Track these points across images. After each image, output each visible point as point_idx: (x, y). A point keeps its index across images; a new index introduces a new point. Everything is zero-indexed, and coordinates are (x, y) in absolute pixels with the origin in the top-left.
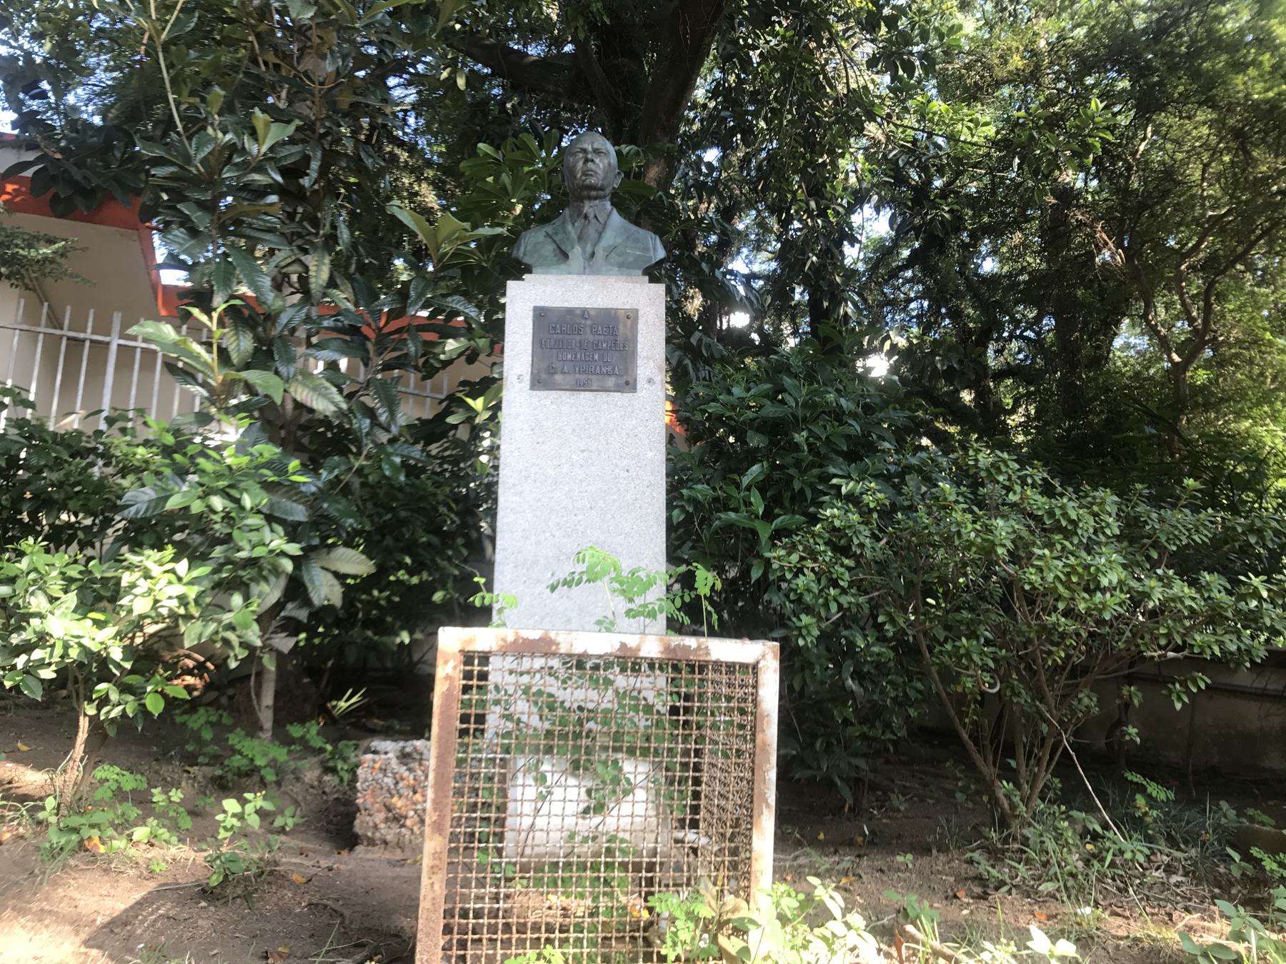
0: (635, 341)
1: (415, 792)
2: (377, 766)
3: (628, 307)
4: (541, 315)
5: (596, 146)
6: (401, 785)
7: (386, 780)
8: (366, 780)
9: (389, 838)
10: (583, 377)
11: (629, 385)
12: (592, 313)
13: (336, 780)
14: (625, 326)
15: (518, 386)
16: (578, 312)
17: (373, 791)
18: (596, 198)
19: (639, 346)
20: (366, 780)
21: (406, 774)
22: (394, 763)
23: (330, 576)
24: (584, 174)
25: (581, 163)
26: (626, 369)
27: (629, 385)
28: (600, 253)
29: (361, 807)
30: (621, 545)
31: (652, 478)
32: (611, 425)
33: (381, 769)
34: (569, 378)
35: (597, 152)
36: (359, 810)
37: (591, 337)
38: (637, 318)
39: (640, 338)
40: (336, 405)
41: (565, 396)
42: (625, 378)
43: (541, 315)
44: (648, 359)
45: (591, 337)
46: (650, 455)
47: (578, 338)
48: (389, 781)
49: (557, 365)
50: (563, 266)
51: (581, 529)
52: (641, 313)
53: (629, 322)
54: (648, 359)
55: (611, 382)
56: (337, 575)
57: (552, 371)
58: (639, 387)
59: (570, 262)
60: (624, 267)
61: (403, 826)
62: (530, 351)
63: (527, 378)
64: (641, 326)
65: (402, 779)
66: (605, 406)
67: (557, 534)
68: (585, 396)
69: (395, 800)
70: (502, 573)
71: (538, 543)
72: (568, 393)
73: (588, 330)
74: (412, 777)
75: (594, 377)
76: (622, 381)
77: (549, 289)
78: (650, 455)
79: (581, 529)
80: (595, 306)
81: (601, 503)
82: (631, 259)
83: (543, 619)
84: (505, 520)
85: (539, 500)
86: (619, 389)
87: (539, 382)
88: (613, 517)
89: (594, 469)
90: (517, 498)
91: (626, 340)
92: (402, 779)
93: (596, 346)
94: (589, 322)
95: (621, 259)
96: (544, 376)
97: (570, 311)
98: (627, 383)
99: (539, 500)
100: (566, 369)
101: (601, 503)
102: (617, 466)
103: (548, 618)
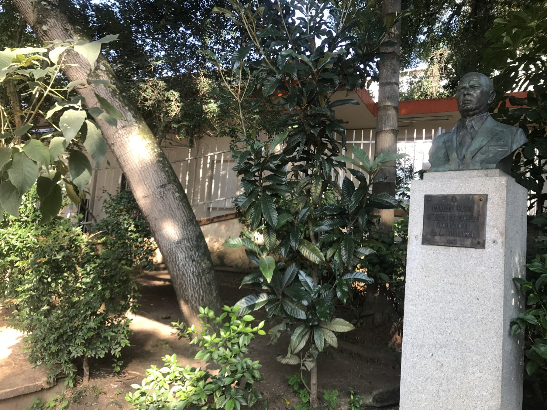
0: (484, 215)
3: (481, 193)
4: (428, 199)
5: (472, 83)
10: (451, 238)
11: (480, 244)
12: (458, 198)
14: (478, 206)
15: (415, 242)
16: (450, 198)
18: (473, 115)
19: (488, 219)
23: (331, 333)
24: (464, 103)
25: (462, 97)
26: (479, 234)
27: (480, 244)
28: (468, 156)
31: (494, 306)
32: (468, 269)
34: (444, 239)
35: (473, 87)
37: (457, 213)
38: (486, 200)
39: (488, 213)
40: (320, 258)
41: (441, 249)
42: (477, 240)
43: (428, 199)
44: (493, 227)
45: (457, 213)
46: (493, 291)
47: (449, 214)
49: (437, 230)
50: (447, 166)
52: (489, 197)
53: (481, 203)
54: (494, 227)
55: (469, 242)
56: (333, 332)
57: (433, 234)
58: (486, 245)
59: (451, 162)
60: (485, 165)
62: (422, 222)
63: (420, 237)
64: (489, 205)
66: (465, 257)
68: (453, 250)
70: (406, 348)
72: (443, 247)
73: (455, 209)
75: (458, 239)
76: (475, 242)
77: (434, 184)
78: (493, 291)
80: (460, 193)
81: (461, 317)
82: (491, 155)
83: (427, 379)
85: (425, 310)
86: (473, 246)
87: (428, 239)
88: (468, 327)
89: (457, 295)
90: (412, 307)
91: (479, 215)
93: (460, 218)
94: (456, 204)
95: (483, 157)
96: (429, 237)
97: (445, 197)
98: (479, 243)
99: (425, 310)
100: (441, 234)
101: (461, 317)
102: (471, 295)
103: (429, 380)
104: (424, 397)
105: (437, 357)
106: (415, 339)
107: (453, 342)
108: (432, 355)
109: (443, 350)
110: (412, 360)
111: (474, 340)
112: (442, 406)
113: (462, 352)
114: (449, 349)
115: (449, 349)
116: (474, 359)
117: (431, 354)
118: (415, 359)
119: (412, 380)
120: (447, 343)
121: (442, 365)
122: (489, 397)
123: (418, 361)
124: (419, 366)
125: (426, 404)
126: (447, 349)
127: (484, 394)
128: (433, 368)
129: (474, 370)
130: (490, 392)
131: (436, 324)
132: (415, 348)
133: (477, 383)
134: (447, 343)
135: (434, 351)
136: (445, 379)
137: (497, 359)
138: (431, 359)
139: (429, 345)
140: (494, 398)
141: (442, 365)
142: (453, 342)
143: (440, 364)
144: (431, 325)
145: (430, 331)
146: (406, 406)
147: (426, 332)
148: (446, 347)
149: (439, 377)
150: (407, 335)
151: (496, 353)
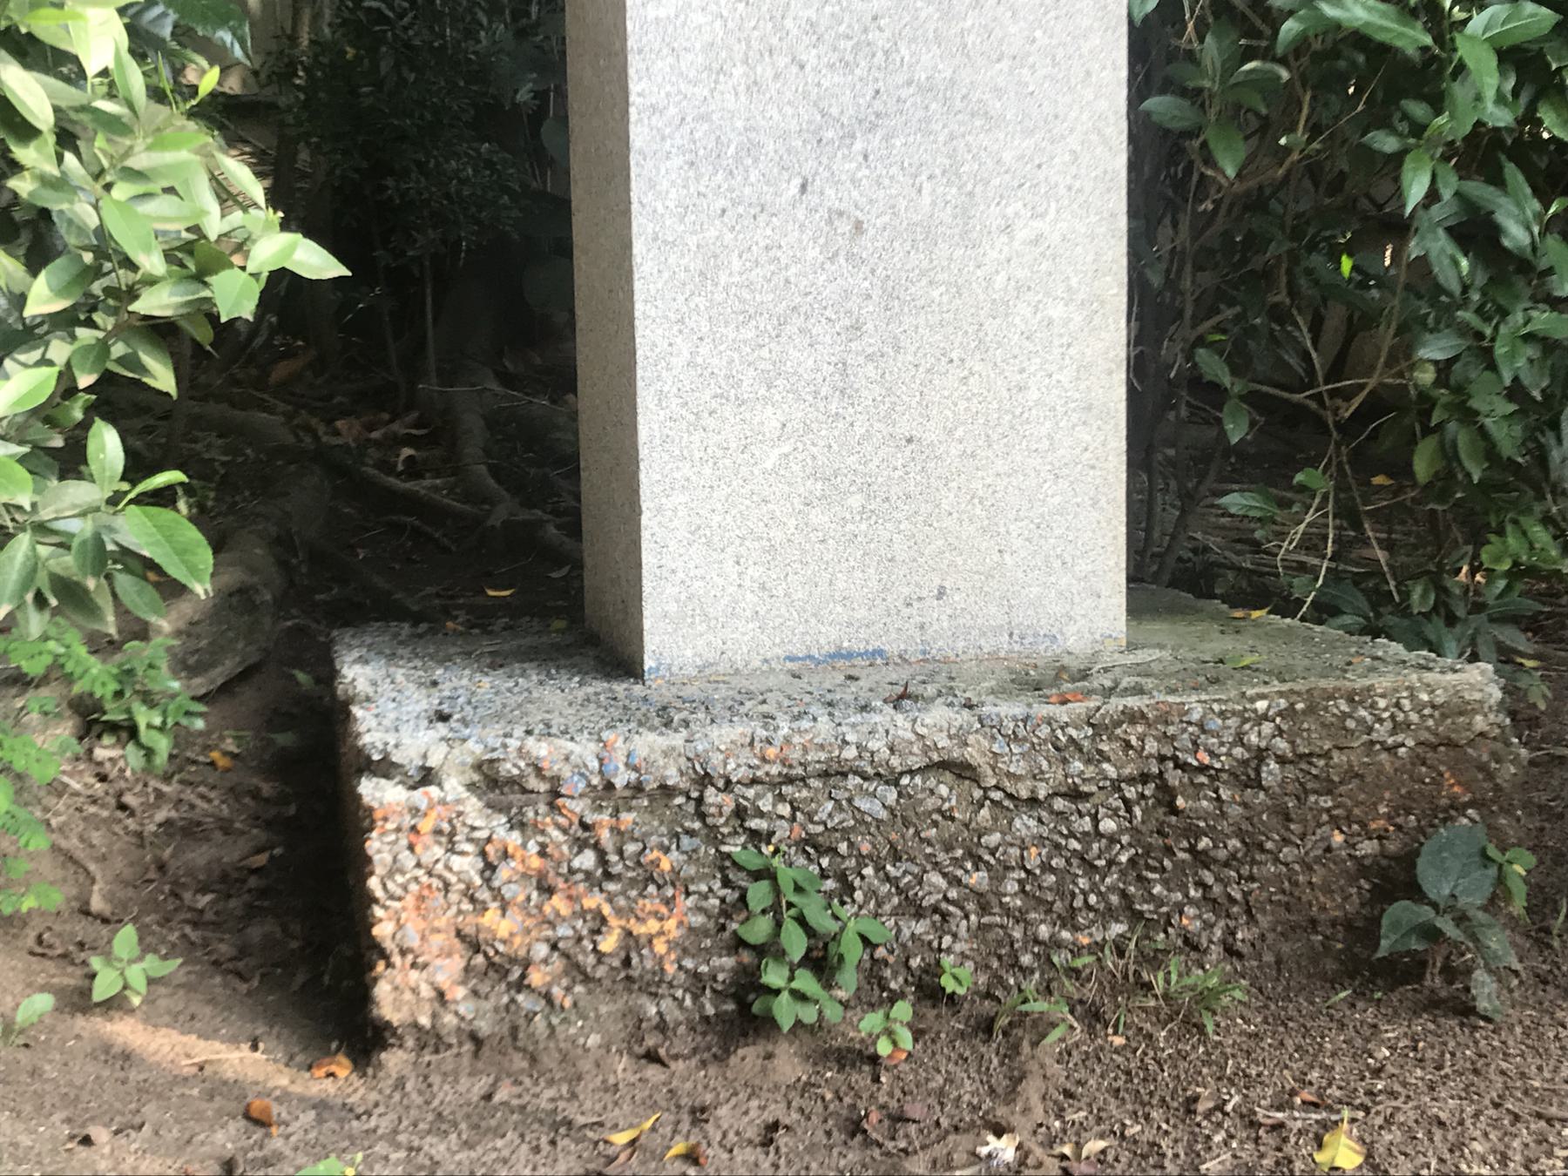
1: (547, 890)
2: (426, 825)
6: (504, 873)
7: (457, 862)
8: (395, 869)
9: (484, 1027)
13: (133, 757)
17: (421, 898)
20: (395, 869)
21: (515, 838)
22: (473, 806)
29: (389, 945)
30: (998, 92)
33: (438, 832)
36: (384, 955)
48: (467, 865)
51: (880, 40)
61: (521, 985)
65: (506, 855)
67: (810, 57)
69: (491, 918)
70: (652, 184)
71: (754, 86)
74: (533, 847)
79: (880, 40)
84: (651, 12)
92: (506, 855)
104: (770, 419)
105: (830, 192)
106: (704, 118)
107: (904, 93)
108: (804, 188)
109: (858, 146)
110: (692, 241)
111: (1004, 65)
112: (867, 436)
113: (952, 137)
114: (887, 138)
115: (887, 138)
116: (1007, 156)
117: (797, 181)
118: (713, 233)
119: (704, 349)
120: (878, 105)
121: (858, 227)
122: (1078, 318)
123: (728, 237)
124: (736, 265)
125: (786, 449)
126: (876, 139)
127: (1057, 311)
128: (813, 253)
129: (1010, 211)
130: (1081, 296)
131: (811, 13)
132: (706, 169)
133: (1021, 274)
134: (878, 105)
135: (808, 168)
136: (876, 293)
137: (1108, 131)
138: (801, 214)
139: (785, 136)
140: (1097, 320)
141: (858, 227)
142: (904, 93)
143: (845, 227)
144: (789, 23)
145: (782, 61)
146: (679, 498)
147: (765, 71)
148: (873, 128)
149: (847, 294)
150: (654, 108)
151: (1103, 105)
